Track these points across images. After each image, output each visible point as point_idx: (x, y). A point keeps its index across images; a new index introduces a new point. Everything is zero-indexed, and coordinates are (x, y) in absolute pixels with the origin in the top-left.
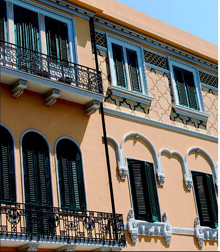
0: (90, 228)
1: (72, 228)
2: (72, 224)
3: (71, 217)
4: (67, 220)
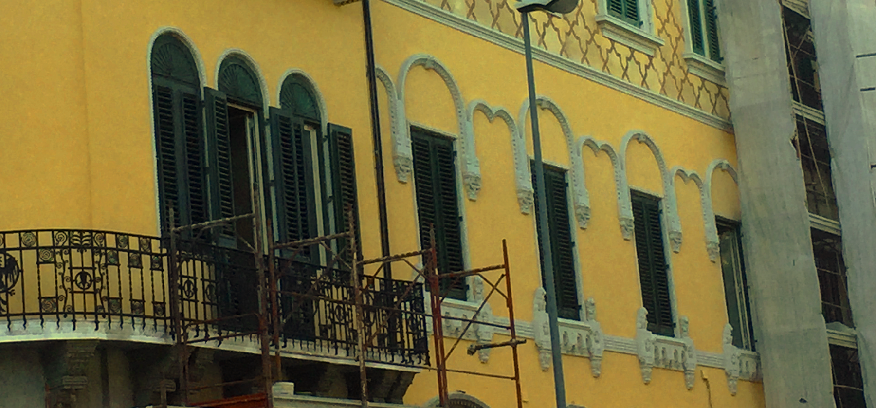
3: (82, 253)
4: (67, 265)
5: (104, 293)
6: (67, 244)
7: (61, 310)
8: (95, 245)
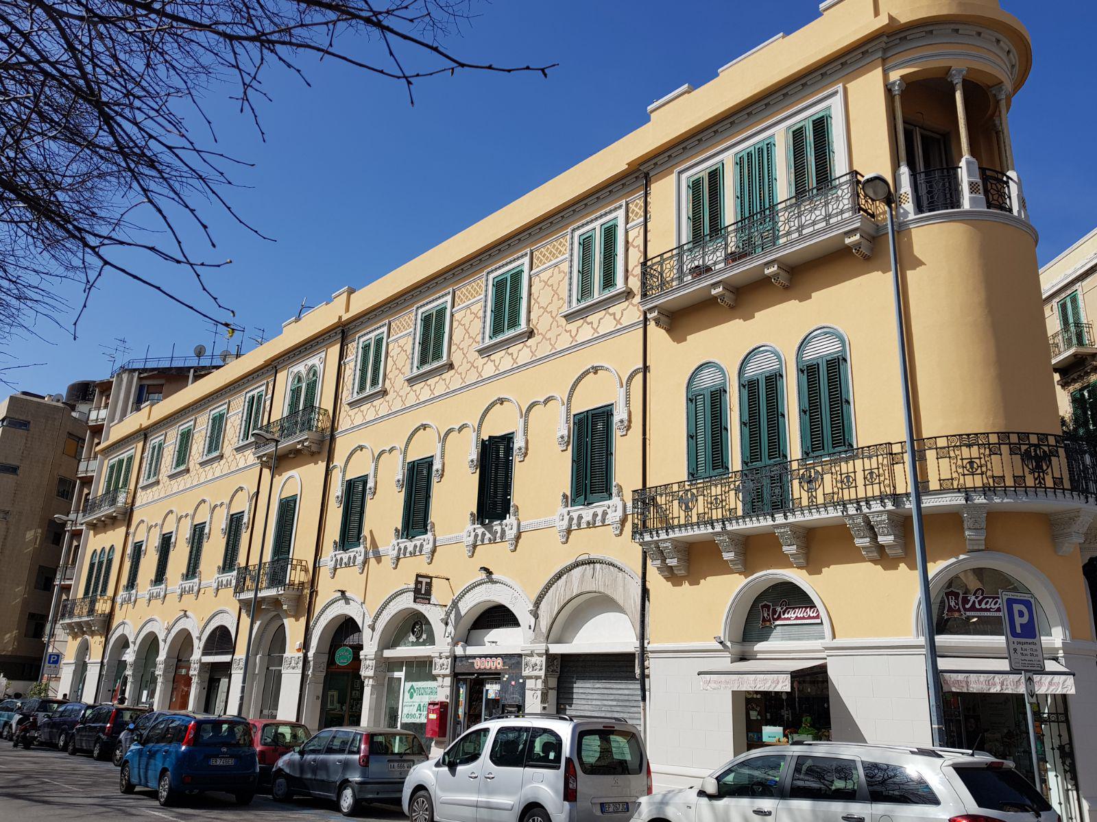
0: (1038, 468)
2: (971, 463)
4: (959, 457)
5: (989, 473)
6: (958, 444)
8: (980, 442)
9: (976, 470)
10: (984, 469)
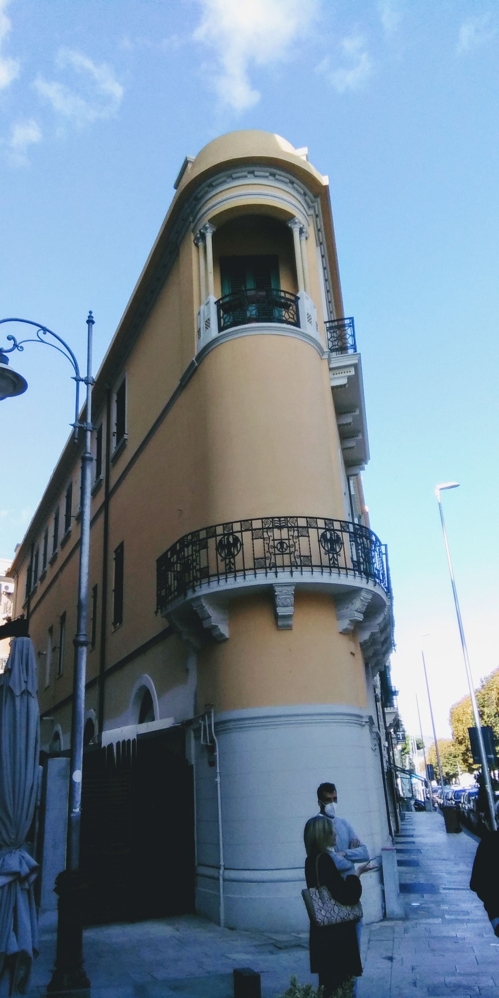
1: (284, 550)
2: (282, 543)
4: (271, 538)
5: (297, 553)
6: (271, 526)
7: (267, 565)
8: (289, 525)
9: (286, 550)
10: (292, 549)
